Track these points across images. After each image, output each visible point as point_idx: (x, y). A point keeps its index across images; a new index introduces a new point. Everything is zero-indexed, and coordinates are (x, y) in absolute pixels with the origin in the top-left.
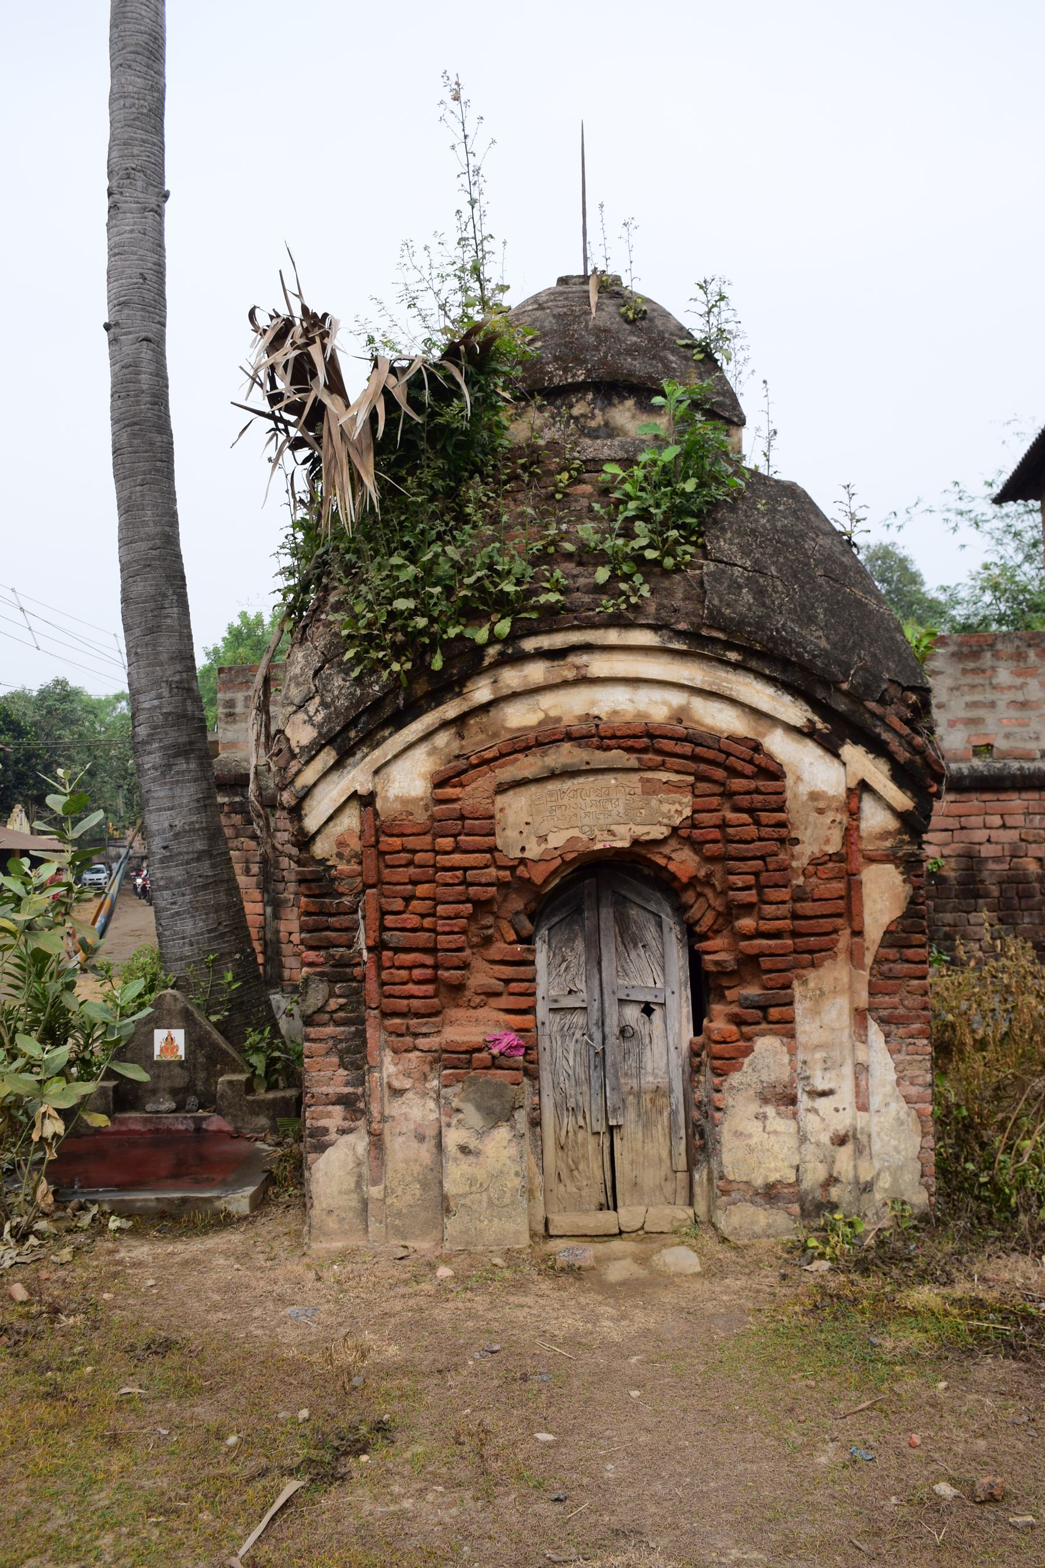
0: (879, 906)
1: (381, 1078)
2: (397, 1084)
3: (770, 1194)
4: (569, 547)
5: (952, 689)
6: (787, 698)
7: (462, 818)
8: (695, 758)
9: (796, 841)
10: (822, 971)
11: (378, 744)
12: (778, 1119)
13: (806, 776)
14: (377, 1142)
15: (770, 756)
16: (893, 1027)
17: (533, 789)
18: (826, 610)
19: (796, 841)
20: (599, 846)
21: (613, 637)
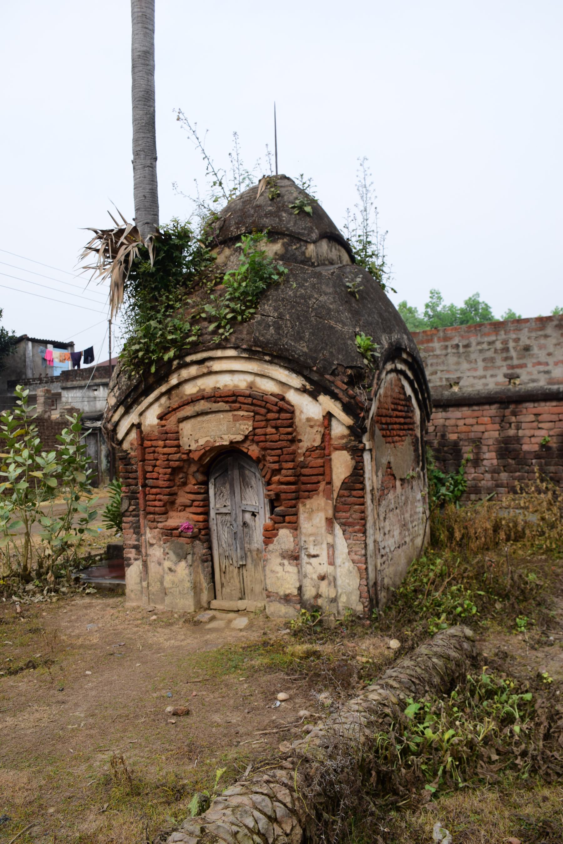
0: (340, 471)
1: (146, 539)
2: (151, 542)
3: (286, 599)
4: (203, 315)
5: (556, 345)
6: (294, 375)
7: (167, 433)
8: (252, 404)
9: (300, 441)
10: (312, 500)
11: (140, 403)
12: (289, 566)
13: (305, 411)
14: (145, 564)
15: (288, 403)
16: (347, 527)
17: (193, 421)
18: (310, 333)
19: (300, 441)
20: (217, 444)
21: (219, 353)
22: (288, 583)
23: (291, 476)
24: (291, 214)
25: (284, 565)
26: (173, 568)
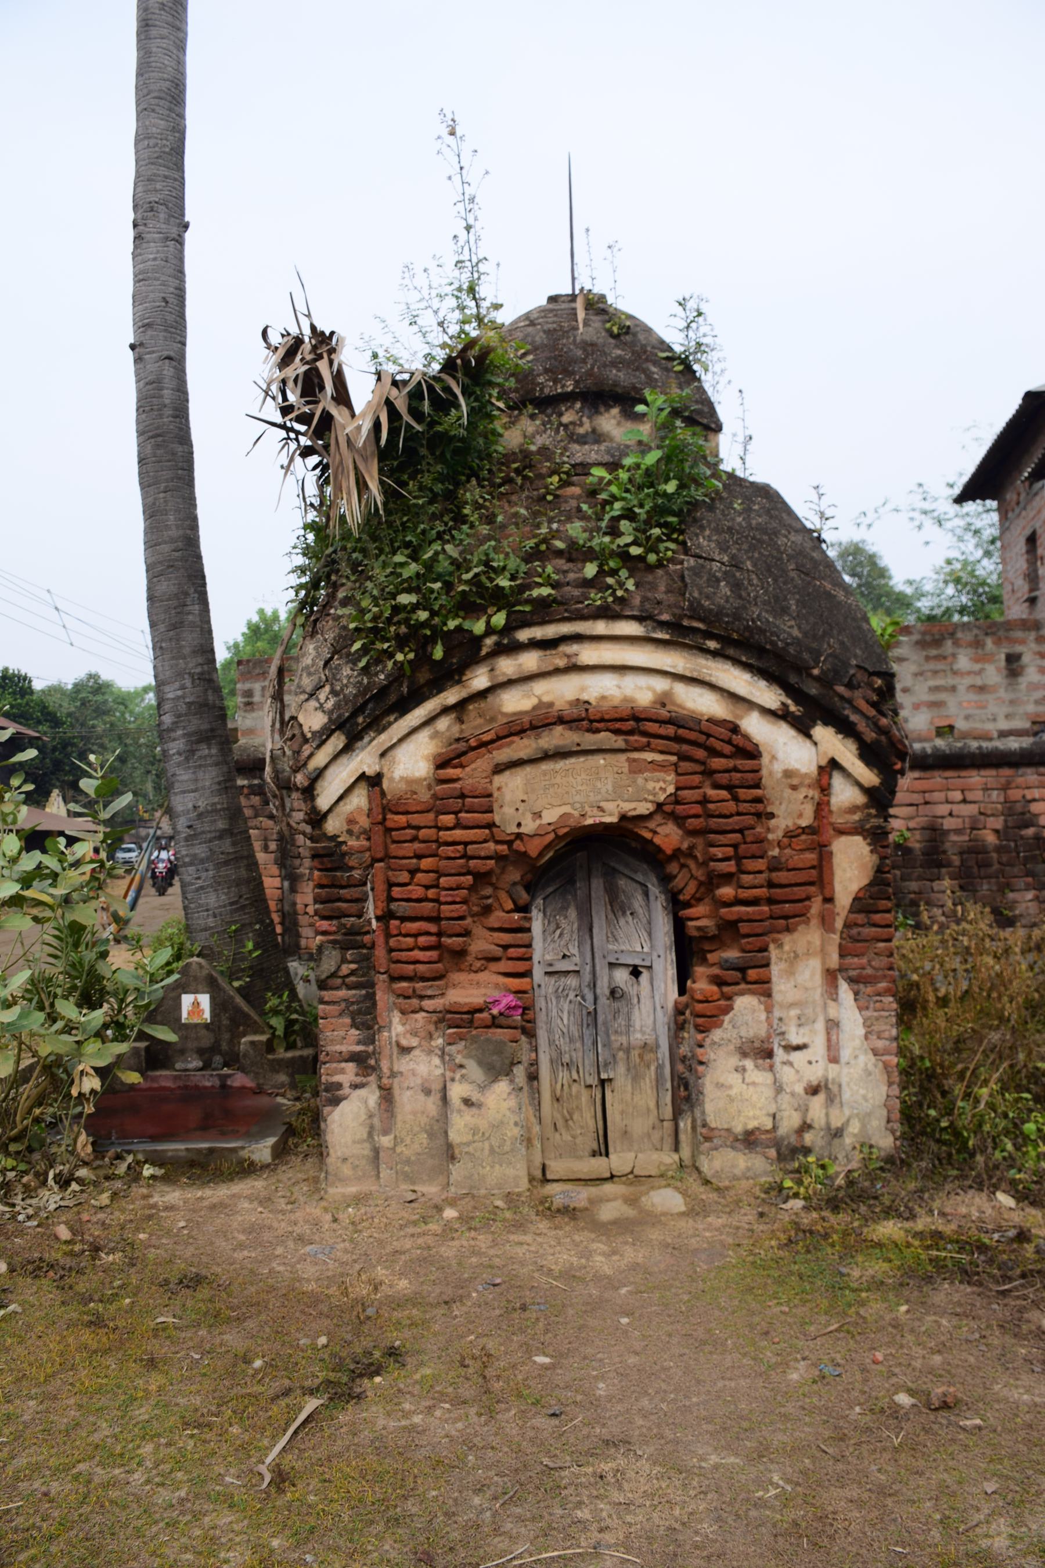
0: (848, 875)
1: (390, 1037)
2: (404, 1043)
3: (749, 1140)
4: (559, 544)
5: (916, 675)
6: (763, 684)
7: (463, 796)
8: (677, 739)
9: (772, 816)
10: (796, 935)
11: (384, 729)
12: (756, 1072)
13: (780, 755)
14: (387, 1096)
15: (747, 737)
16: (861, 986)
17: (528, 769)
18: (798, 601)
19: (772, 816)
20: (589, 821)
21: (600, 627)
22: (754, 1106)
23: (761, 887)
24: (668, 370)
25: (744, 1070)
26: (475, 1097)
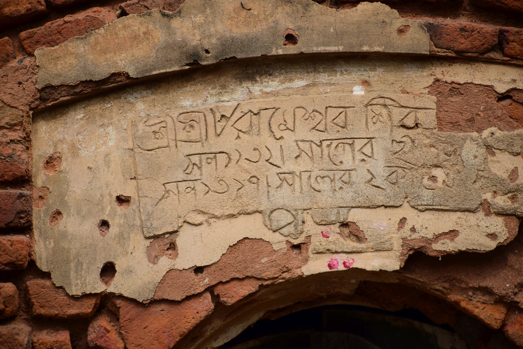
17: (141, 107)
20: (317, 266)
